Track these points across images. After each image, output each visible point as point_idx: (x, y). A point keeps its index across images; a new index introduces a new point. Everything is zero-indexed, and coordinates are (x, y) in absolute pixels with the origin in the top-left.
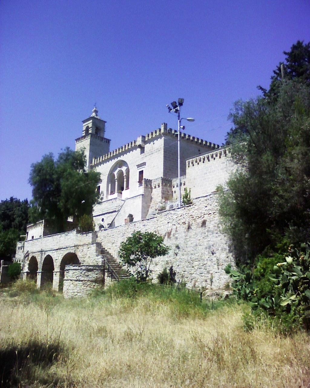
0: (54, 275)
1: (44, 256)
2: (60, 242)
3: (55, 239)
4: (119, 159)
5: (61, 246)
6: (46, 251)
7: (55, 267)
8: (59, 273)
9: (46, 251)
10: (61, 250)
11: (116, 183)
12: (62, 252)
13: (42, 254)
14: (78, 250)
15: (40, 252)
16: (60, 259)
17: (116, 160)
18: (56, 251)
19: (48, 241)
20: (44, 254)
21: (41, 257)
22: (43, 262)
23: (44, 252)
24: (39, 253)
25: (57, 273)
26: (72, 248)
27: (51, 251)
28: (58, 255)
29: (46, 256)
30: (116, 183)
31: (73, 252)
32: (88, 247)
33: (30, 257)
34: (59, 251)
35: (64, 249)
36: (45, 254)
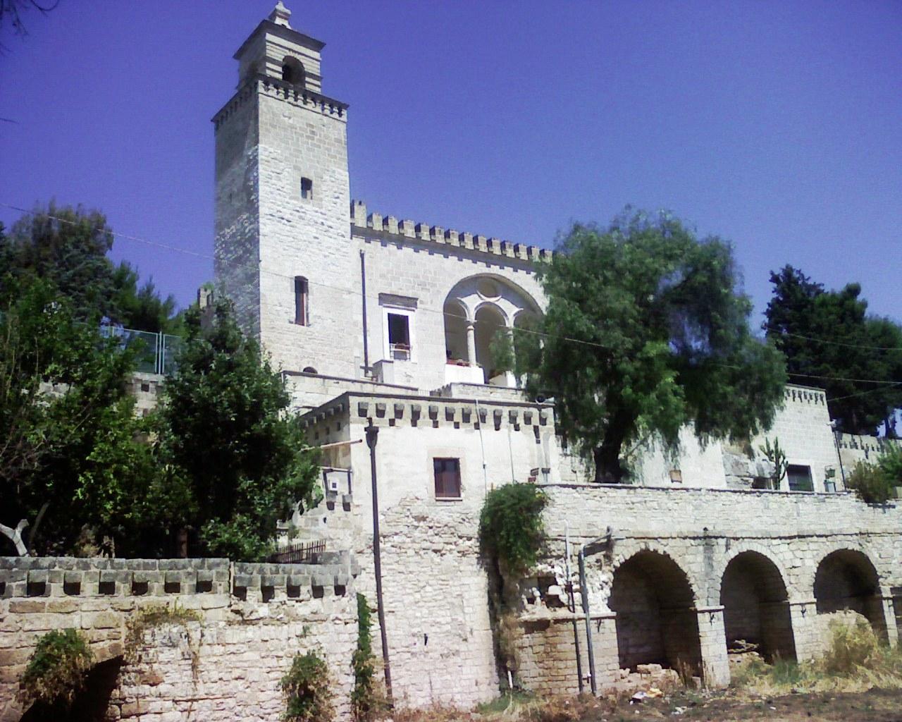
0: (795, 612)
1: (723, 558)
4: (495, 270)
5: (806, 529)
6: (737, 539)
7: (789, 588)
9: (737, 539)
10: (809, 539)
11: (471, 334)
12: (812, 546)
13: (709, 548)
15: (694, 538)
16: (811, 566)
17: (480, 268)
18: (788, 541)
20: (724, 549)
21: (709, 560)
22: (720, 571)
23: (722, 542)
24: (692, 541)
25: (808, 607)
26: (849, 538)
28: (799, 554)
29: (733, 553)
30: (471, 334)
31: (857, 548)
33: (623, 553)
34: (802, 544)
35: (824, 539)
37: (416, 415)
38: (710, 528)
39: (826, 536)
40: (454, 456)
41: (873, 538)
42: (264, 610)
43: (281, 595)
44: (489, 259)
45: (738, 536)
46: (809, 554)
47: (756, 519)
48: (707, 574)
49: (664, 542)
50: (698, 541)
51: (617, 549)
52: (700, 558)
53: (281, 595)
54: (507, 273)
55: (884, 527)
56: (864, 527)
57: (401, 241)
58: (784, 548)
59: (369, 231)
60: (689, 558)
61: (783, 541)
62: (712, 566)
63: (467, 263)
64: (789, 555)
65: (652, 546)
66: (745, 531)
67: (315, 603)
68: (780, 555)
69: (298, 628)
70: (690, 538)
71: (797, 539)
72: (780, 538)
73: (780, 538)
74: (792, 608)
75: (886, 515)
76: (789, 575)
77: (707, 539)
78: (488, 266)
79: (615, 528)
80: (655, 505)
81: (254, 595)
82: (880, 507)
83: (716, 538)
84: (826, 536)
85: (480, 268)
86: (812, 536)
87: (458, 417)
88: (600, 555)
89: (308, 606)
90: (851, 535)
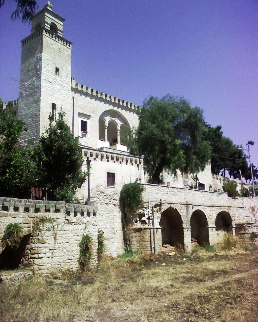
0: (210, 230)
1: (191, 211)
2: (212, 199)
3: (206, 196)
4: (116, 108)
5: (214, 204)
6: (195, 205)
7: (208, 222)
8: (215, 228)
9: (195, 205)
10: (215, 207)
11: (106, 130)
12: (215, 209)
13: (188, 208)
14: (230, 210)
15: (184, 204)
16: (215, 216)
17: (110, 107)
18: (209, 207)
19: (196, 195)
20: (191, 208)
21: (187, 211)
22: (190, 216)
23: (191, 206)
24: (183, 205)
25: (213, 228)
26: (225, 208)
27: (203, 207)
28: (212, 212)
29: (194, 210)
30: (106, 130)
31: (227, 211)
32: (237, 209)
33: (165, 207)
35: (218, 207)
36: (193, 208)
37: (102, 157)
38: (188, 201)
39: (219, 207)
40: (113, 172)
41: (231, 208)
42: (74, 220)
43: (79, 215)
44: (114, 104)
45: (196, 205)
46: (214, 212)
47: (201, 200)
48: (187, 216)
49: (175, 205)
50: (185, 205)
51: (163, 207)
52: (185, 211)
53: (79, 215)
54: (119, 110)
55: (234, 205)
56: (230, 205)
57: (86, 94)
58: (208, 209)
59: (76, 89)
60: (182, 211)
61: (208, 207)
62: (188, 214)
63: (107, 105)
64: (209, 212)
65: (173, 206)
66: (197, 203)
67: (88, 218)
68: (207, 212)
69: (83, 226)
70: (183, 204)
71: (211, 207)
72: (207, 206)
73: (207, 206)
74: (209, 229)
75: (235, 201)
76: (208, 218)
77: (187, 205)
78: (114, 107)
79: (163, 200)
80: (174, 193)
81: (72, 214)
82: (233, 199)
83: (190, 205)
84: (219, 207)
85: (110, 107)
86: (215, 206)
87: (115, 159)
88: (158, 208)
89: (86, 219)
90: (226, 207)
